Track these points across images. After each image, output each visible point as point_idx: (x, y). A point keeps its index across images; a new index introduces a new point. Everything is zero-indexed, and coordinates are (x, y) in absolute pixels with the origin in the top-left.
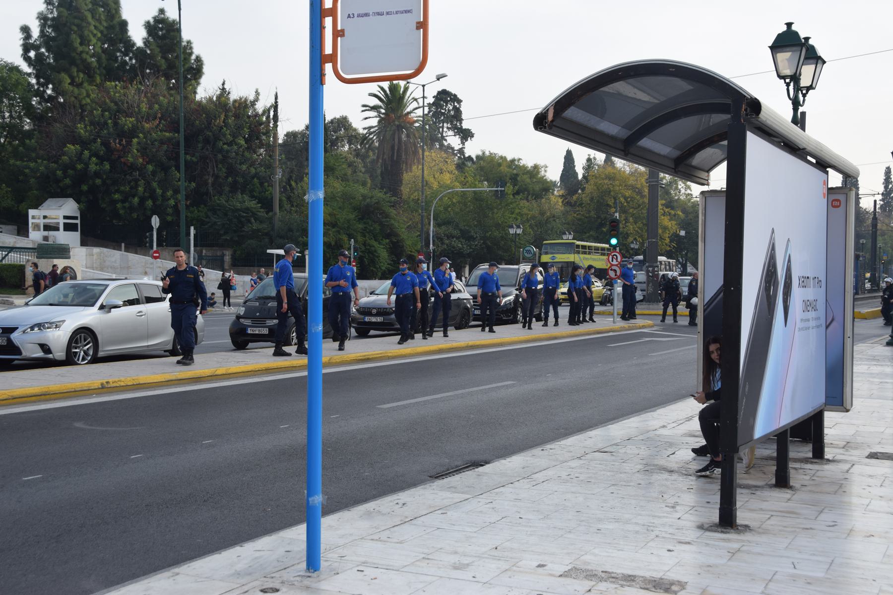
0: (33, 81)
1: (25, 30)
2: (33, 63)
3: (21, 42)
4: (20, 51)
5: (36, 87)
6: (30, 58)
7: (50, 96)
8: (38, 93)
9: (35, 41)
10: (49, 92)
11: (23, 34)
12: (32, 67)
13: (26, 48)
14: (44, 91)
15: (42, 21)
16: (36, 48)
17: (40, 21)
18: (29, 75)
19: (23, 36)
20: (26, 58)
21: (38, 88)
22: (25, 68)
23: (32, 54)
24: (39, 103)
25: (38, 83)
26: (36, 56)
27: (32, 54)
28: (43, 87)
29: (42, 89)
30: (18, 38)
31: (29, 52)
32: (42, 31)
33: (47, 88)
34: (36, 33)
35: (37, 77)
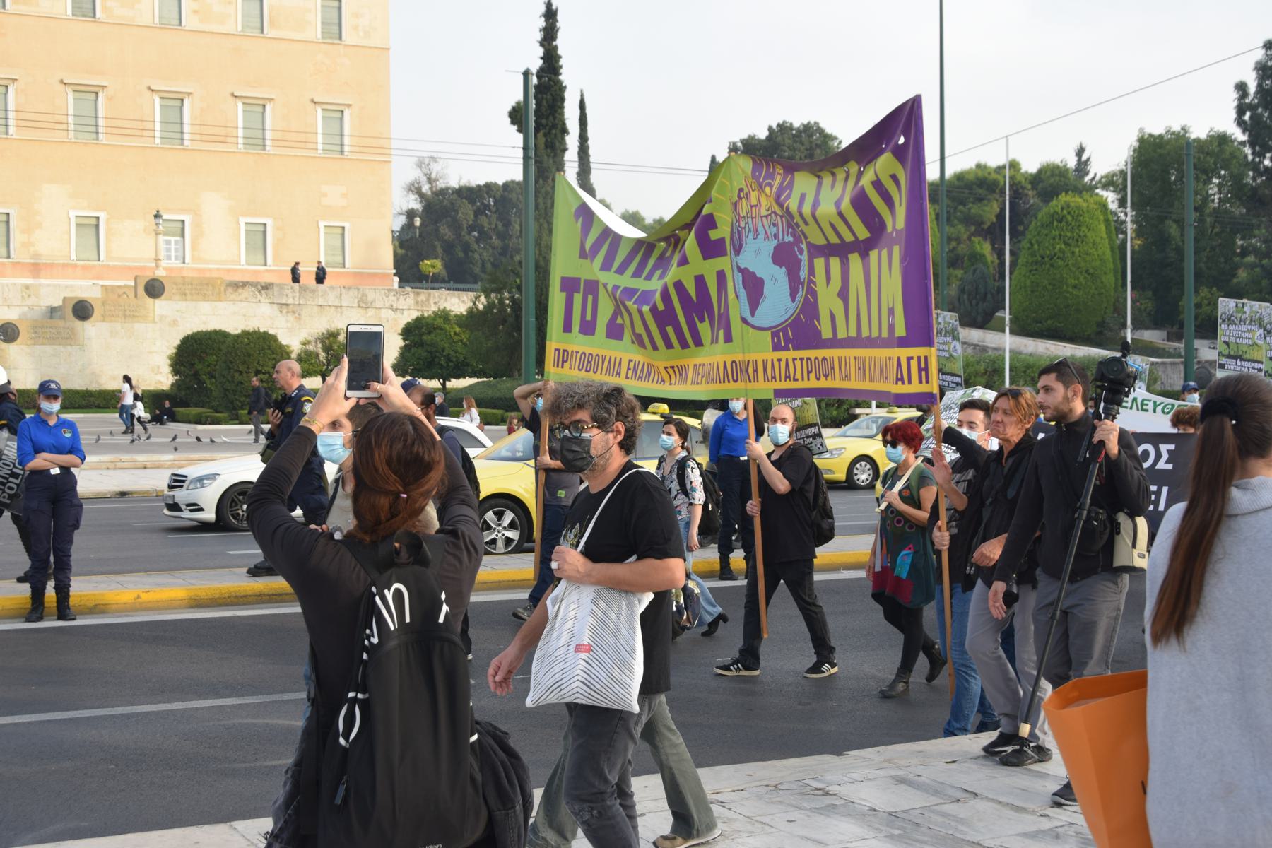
0: (1248, 150)
1: (1241, 87)
2: (1249, 128)
3: (1235, 103)
4: (1233, 115)
5: (1250, 158)
6: (1245, 122)
7: (1266, 168)
8: (1255, 167)
9: (1253, 100)
10: (1267, 162)
11: (1238, 92)
12: (1247, 134)
13: (1241, 110)
14: (1261, 162)
15: (1260, 72)
16: (1251, 107)
17: (1258, 73)
18: (1243, 143)
19: (1237, 96)
20: (1240, 122)
21: (1253, 159)
22: (1240, 136)
23: (1247, 116)
24: (1254, 179)
25: (1253, 153)
26: (1251, 117)
27: (1247, 116)
28: (1259, 157)
29: (1257, 160)
30: (1231, 99)
31: (1244, 114)
32: (1259, 85)
33: (1264, 157)
34: (1252, 87)
35: (1252, 143)
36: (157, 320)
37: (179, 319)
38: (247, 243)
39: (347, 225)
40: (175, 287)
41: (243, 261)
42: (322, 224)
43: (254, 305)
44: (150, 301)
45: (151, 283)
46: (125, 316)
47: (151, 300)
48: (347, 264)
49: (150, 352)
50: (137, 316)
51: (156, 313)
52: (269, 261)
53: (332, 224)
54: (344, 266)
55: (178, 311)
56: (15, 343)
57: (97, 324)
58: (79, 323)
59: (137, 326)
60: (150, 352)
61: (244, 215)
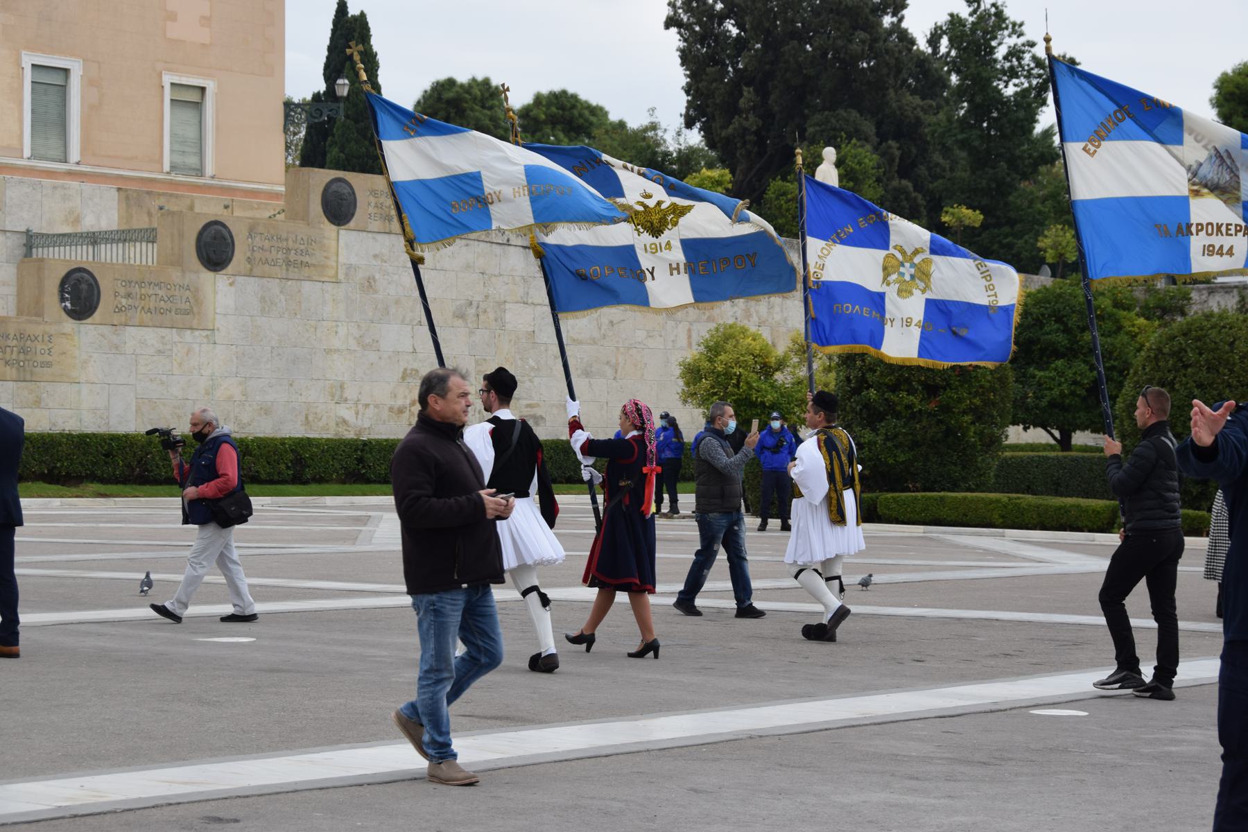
36: (341, 277)
37: (377, 276)
38: (33, 111)
39: (211, 86)
40: (372, 199)
41: (27, 152)
42: (167, 79)
43: (497, 249)
44: (329, 229)
45: (334, 187)
46: (288, 263)
47: (334, 227)
48: (209, 169)
49: (329, 351)
50: (307, 265)
51: (341, 259)
52: (75, 153)
53: (184, 81)
54: (200, 171)
55: (375, 256)
56: (89, 320)
57: (240, 279)
58: (207, 276)
59: (307, 286)
60: (329, 351)
61: (33, 48)
